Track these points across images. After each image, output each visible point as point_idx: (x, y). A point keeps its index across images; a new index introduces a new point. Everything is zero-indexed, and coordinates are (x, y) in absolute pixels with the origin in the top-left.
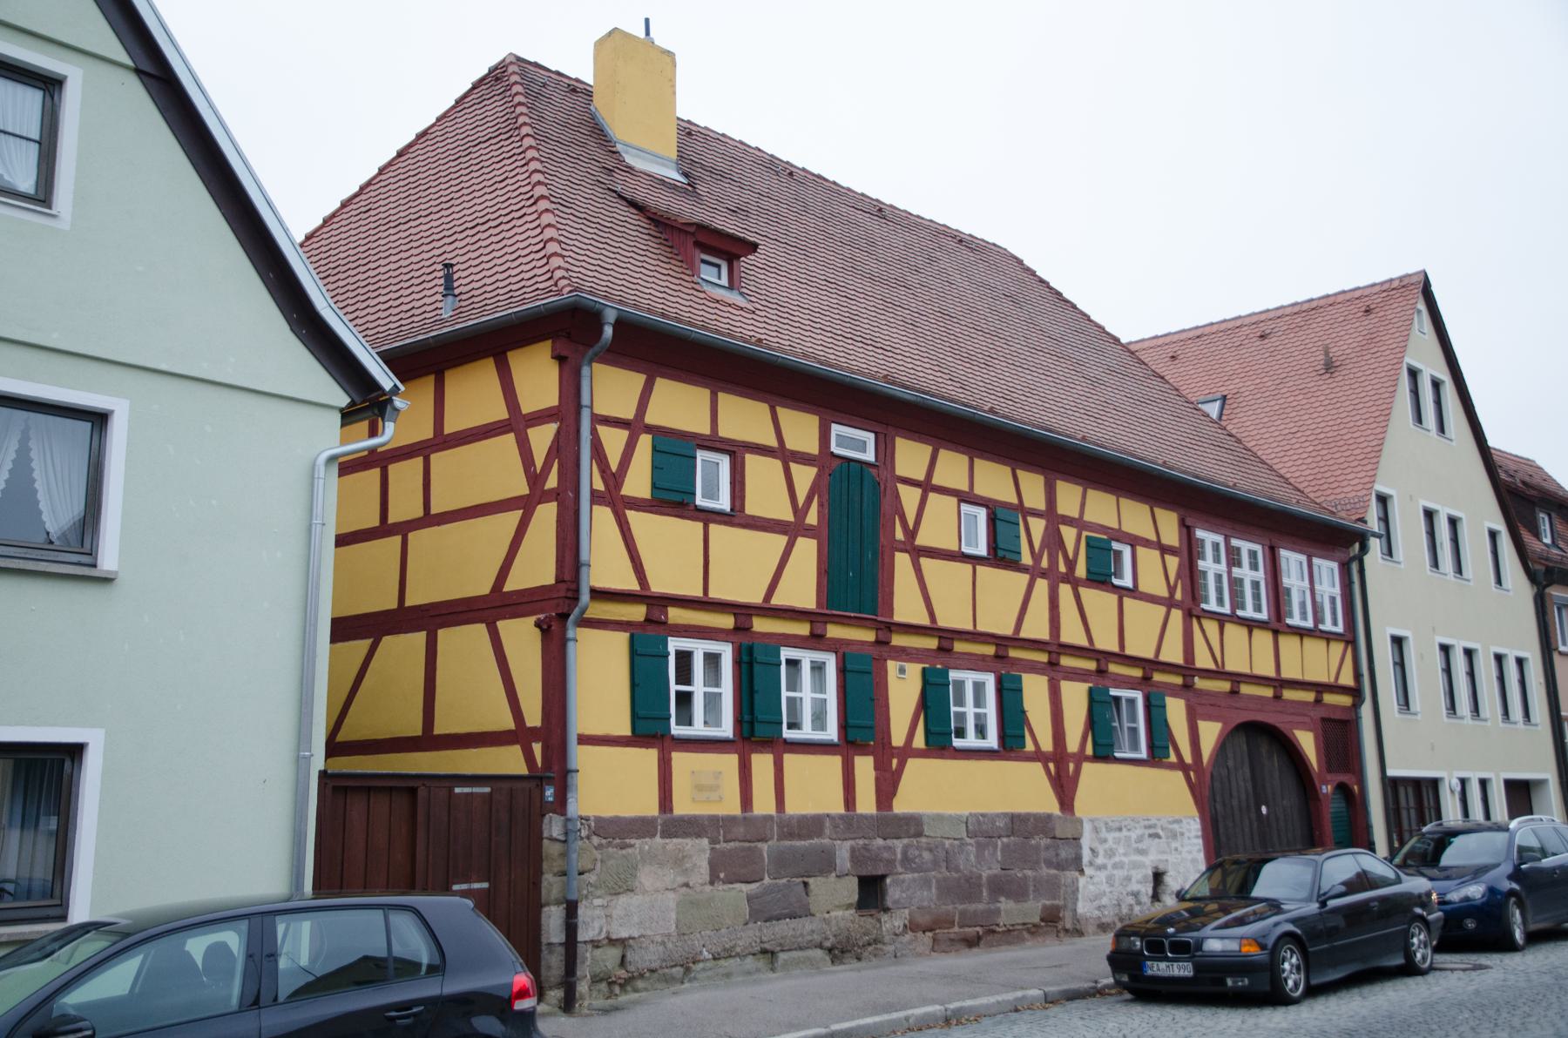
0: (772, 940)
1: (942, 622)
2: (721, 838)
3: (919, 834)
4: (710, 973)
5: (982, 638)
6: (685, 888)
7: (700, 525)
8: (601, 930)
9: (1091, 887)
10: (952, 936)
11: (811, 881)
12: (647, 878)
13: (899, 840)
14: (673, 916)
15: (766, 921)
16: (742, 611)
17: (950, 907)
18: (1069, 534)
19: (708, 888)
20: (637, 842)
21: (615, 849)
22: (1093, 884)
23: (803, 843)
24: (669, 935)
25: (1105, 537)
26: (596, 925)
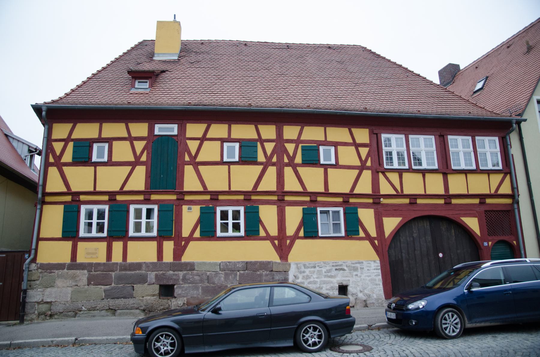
1: (210, 189)
2: (93, 270)
4: (86, 315)
5: (234, 193)
6: (76, 286)
8: (39, 299)
11: (135, 286)
12: (59, 283)
13: (182, 272)
14: (69, 295)
15: (112, 299)
16: (112, 195)
18: (290, 148)
19: (86, 287)
20: (56, 271)
21: (47, 274)
23: (131, 272)
24: (67, 302)
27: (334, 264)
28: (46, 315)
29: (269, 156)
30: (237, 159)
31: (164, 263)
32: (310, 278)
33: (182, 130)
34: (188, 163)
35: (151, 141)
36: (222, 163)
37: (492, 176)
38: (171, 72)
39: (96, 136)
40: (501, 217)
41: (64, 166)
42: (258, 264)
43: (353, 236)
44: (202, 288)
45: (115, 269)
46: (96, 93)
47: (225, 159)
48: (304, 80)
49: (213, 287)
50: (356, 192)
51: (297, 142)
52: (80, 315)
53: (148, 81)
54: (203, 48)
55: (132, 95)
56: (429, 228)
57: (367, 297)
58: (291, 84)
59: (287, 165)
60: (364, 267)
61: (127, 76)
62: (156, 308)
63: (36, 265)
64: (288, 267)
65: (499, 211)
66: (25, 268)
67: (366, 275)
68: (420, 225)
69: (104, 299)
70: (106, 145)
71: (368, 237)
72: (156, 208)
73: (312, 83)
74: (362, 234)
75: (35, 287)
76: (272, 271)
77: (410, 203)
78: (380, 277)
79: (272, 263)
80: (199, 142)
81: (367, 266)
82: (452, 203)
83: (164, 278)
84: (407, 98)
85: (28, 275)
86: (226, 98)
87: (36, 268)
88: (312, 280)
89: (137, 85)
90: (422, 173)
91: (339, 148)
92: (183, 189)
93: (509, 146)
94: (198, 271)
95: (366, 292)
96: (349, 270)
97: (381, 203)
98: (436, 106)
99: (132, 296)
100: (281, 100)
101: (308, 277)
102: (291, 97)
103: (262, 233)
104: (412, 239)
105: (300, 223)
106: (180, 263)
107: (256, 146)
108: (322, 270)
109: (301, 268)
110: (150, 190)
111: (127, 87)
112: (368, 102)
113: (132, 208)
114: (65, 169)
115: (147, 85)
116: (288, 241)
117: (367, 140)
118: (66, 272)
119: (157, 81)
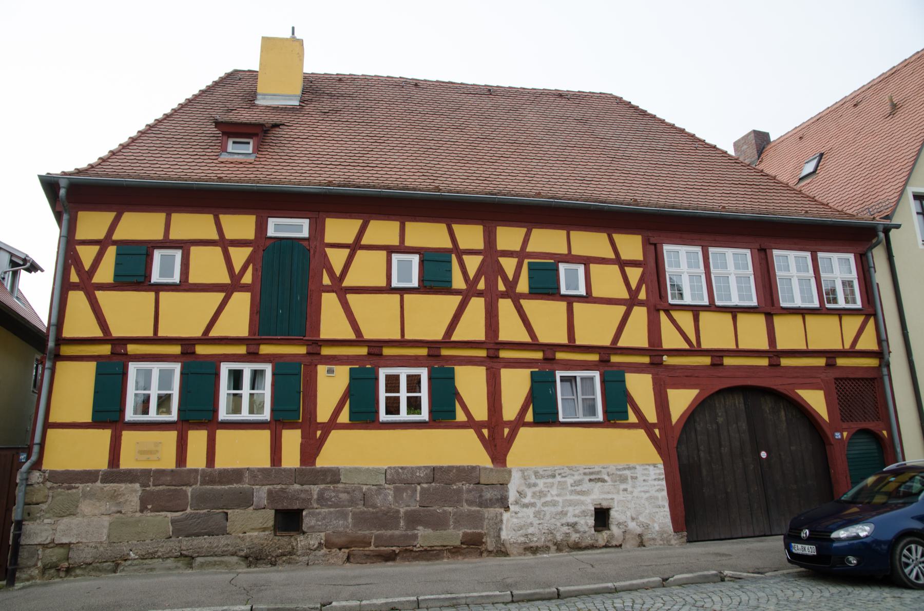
0: (191, 549)
1: (367, 335)
2: (151, 484)
3: (338, 482)
7: (153, 294)
8: (47, 538)
9: (515, 520)
10: (367, 553)
11: (229, 511)
12: (86, 507)
13: (316, 486)
14: (105, 531)
15: (186, 537)
16: (188, 344)
17: (367, 532)
18: (509, 265)
19: (138, 514)
20: (81, 486)
21: (63, 490)
22: (517, 518)
23: (223, 487)
24: (101, 543)
25: (552, 261)
26: (44, 534)
27: (587, 471)
28: (60, 569)
29: (471, 278)
30: (415, 283)
31: (285, 469)
32: (545, 495)
33: (318, 230)
34: (328, 289)
35: (262, 248)
36: (389, 289)
37: (847, 320)
38: (289, 128)
39: (159, 236)
40: (862, 390)
41: (99, 290)
42: (454, 471)
43: (617, 422)
44: (353, 515)
45: (192, 480)
46: (156, 159)
47: (395, 284)
48: (524, 148)
49: (373, 513)
50: (621, 344)
51: (521, 255)
52: (125, 569)
53: (251, 141)
54: (342, 88)
55: (224, 165)
56: (743, 408)
58: (504, 155)
59: (504, 295)
60: (638, 476)
61: (212, 129)
62: (269, 552)
63: (40, 475)
64: (507, 476)
65: (858, 379)
66: (21, 480)
67: (642, 490)
68: (727, 403)
69: (171, 537)
70: (178, 254)
71: (643, 423)
72: (268, 368)
73: (539, 155)
74: (632, 418)
75: (38, 515)
76: (479, 483)
77: (713, 365)
78: (665, 493)
80: (346, 252)
81: (642, 474)
82: (782, 365)
83: (285, 497)
85: (26, 493)
86: (392, 176)
87: (41, 480)
88: (549, 498)
89: (230, 147)
90: (731, 312)
91: (593, 267)
92: (319, 336)
93: (872, 270)
94: (345, 483)
95: (641, 519)
96: (612, 481)
97: (664, 363)
99: (224, 532)
100: (490, 183)
101: (542, 494)
102: (505, 177)
103: (461, 416)
104: (715, 426)
105: (526, 397)
106: (313, 469)
107: (450, 262)
108: (565, 482)
109: (529, 478)
110: (259, 337)
111: (214, 150)
112: (636, 189)
113: (225, 369)
114: (99, 294)
115: (250, 149)
116: (506, 431)
117: (638, 256)
118: (99, 487)
119: (267, 141)
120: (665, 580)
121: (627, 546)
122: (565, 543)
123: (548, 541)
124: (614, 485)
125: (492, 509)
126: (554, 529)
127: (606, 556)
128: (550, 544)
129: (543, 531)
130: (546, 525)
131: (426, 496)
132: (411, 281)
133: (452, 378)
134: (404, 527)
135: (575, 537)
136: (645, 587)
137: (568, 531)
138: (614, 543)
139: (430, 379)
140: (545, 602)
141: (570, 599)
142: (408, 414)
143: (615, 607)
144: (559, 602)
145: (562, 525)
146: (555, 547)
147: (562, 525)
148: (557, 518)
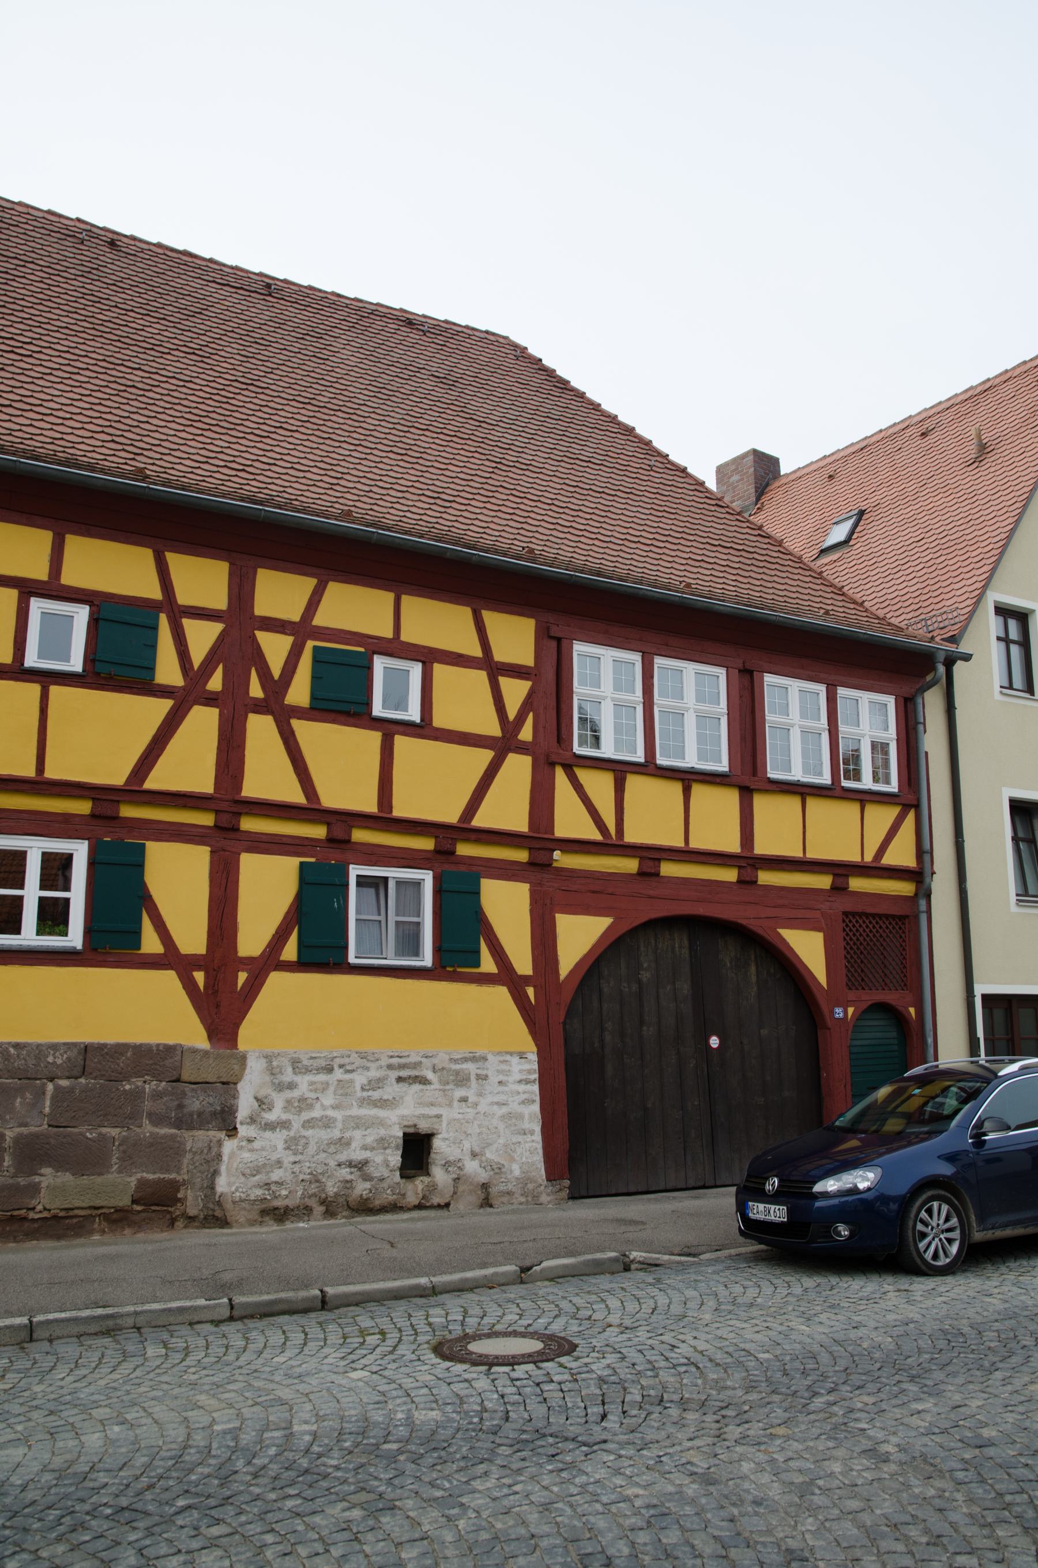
9: (246, 1155)
22: (251, 1150)
25: (362, 650)
29: (196, 665)
30: (76, 664)
32: (311, 1107)
37: (871, 810)
40: (884, 935)
42: (129, 1054)
43: (459, 970)
47: (31, 660)
56: (687, 956)
57: (492, 1173)
59: (259, 707)
60: (490, 1073)
64: (236, 1067)
65: (880, 916)
67: (495, 1100)
68: (660, 946)
71: (506, 975)
74: (488, 964)
76: (178, 1080)
77: (641, 874)
78: (536, 1108)
79: (179, 1052)
81: (498, 1071)
84: (651, 536)
88: (316, 1113)
90: (682, 780)
91: (439, 670)
93: (921, 727)
95: (489, 1155)
96: (440, 1081)
97: (555, 864)
98: (734, 578)
100: (252, 477)
101: (304, 1104)
102: (284, 471)
103: (151, 943)
104: (635, 987)
105: (288, 913)
107: (155, 628)
108: (352, 1081)
109: (281, 1072)
112: (534, 529)
116: (242, 977)
117: (526, 657)
120: (525, 1270)
121: (460, 1206)
122: (341, 1200)
123: (310, 1197)
124: (444, 1091)
125: (201, 1132)
126: (323, 1174)
127: (419, 1225)
128: (313, 1203)
129: (301, 1177)
130: (307, 1164)
131: (65, 1104)
132: (67, 659)
133: (139, 866)
134: (12, 1170)
135: (362, 1188)
136: (488, 1284)
137: (349, 1177)
138: (436, 1200)
139: (93, 864)
140: (295, 1317)
141: (345, 1309)
142: (38, 934)
143: (430, 1324)
144: (324, 1316)
145: (339, 1165)
146: (323, 1208)
147: (339, 1165)
148: (330, 1150)
